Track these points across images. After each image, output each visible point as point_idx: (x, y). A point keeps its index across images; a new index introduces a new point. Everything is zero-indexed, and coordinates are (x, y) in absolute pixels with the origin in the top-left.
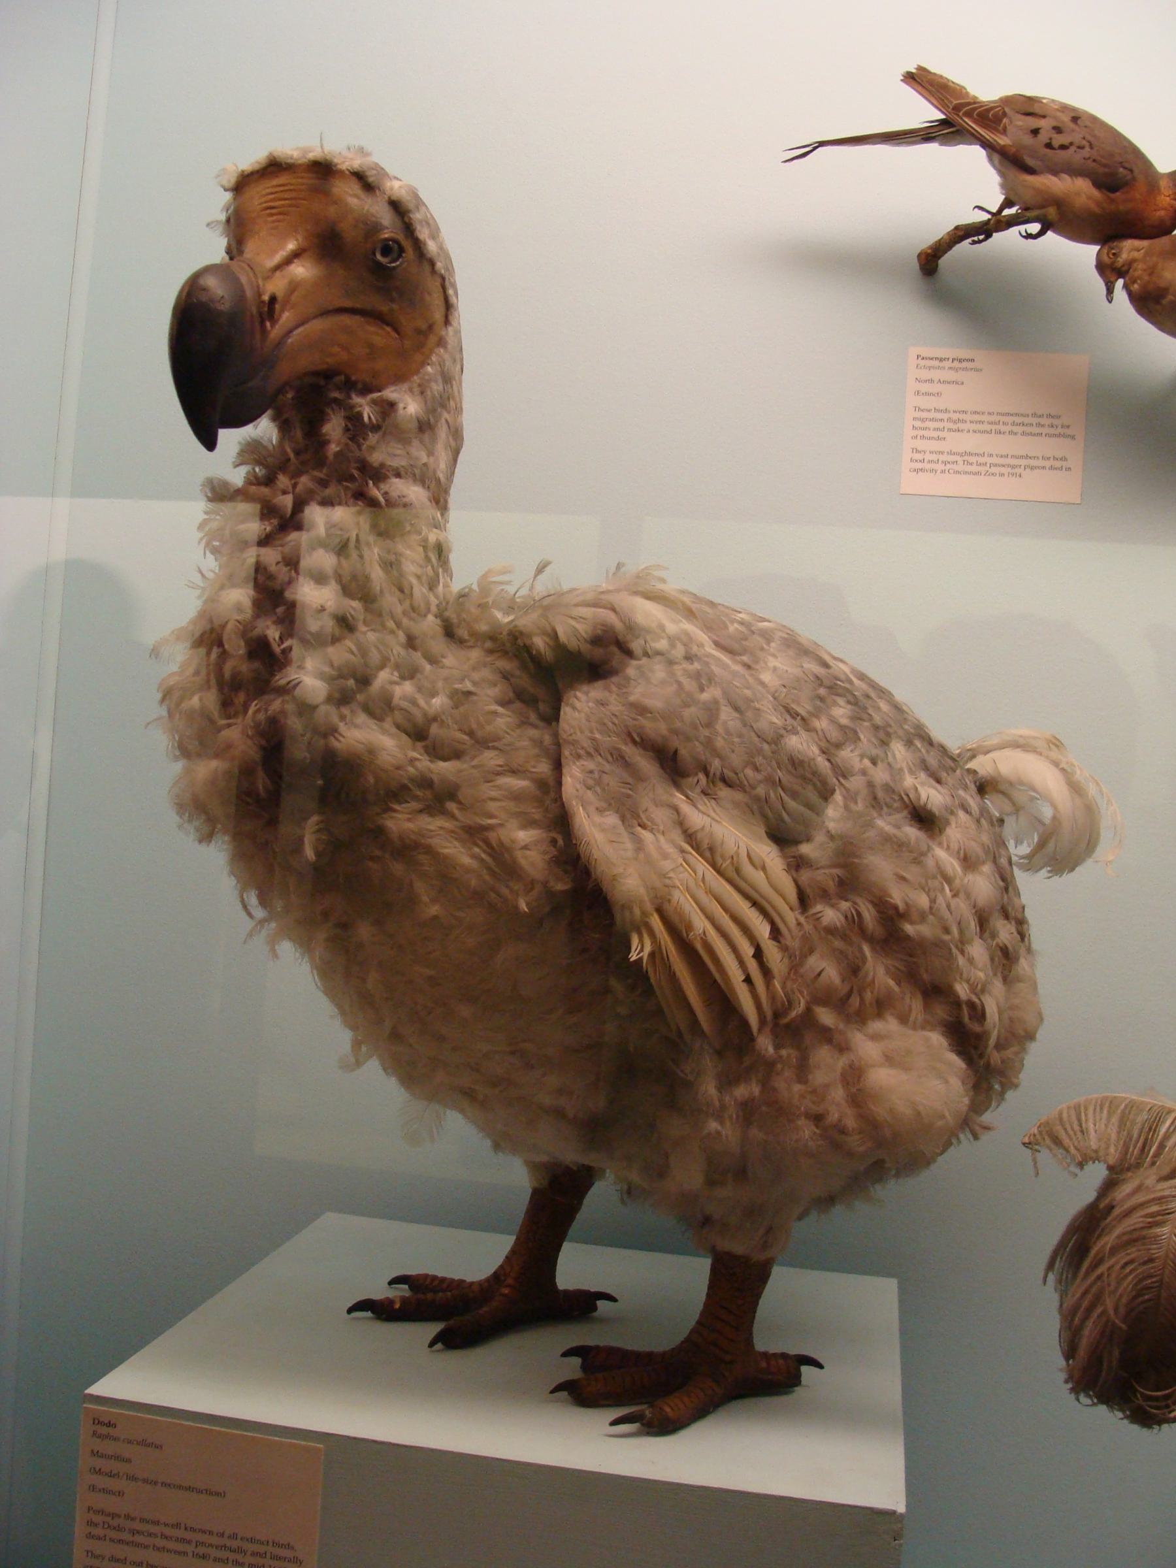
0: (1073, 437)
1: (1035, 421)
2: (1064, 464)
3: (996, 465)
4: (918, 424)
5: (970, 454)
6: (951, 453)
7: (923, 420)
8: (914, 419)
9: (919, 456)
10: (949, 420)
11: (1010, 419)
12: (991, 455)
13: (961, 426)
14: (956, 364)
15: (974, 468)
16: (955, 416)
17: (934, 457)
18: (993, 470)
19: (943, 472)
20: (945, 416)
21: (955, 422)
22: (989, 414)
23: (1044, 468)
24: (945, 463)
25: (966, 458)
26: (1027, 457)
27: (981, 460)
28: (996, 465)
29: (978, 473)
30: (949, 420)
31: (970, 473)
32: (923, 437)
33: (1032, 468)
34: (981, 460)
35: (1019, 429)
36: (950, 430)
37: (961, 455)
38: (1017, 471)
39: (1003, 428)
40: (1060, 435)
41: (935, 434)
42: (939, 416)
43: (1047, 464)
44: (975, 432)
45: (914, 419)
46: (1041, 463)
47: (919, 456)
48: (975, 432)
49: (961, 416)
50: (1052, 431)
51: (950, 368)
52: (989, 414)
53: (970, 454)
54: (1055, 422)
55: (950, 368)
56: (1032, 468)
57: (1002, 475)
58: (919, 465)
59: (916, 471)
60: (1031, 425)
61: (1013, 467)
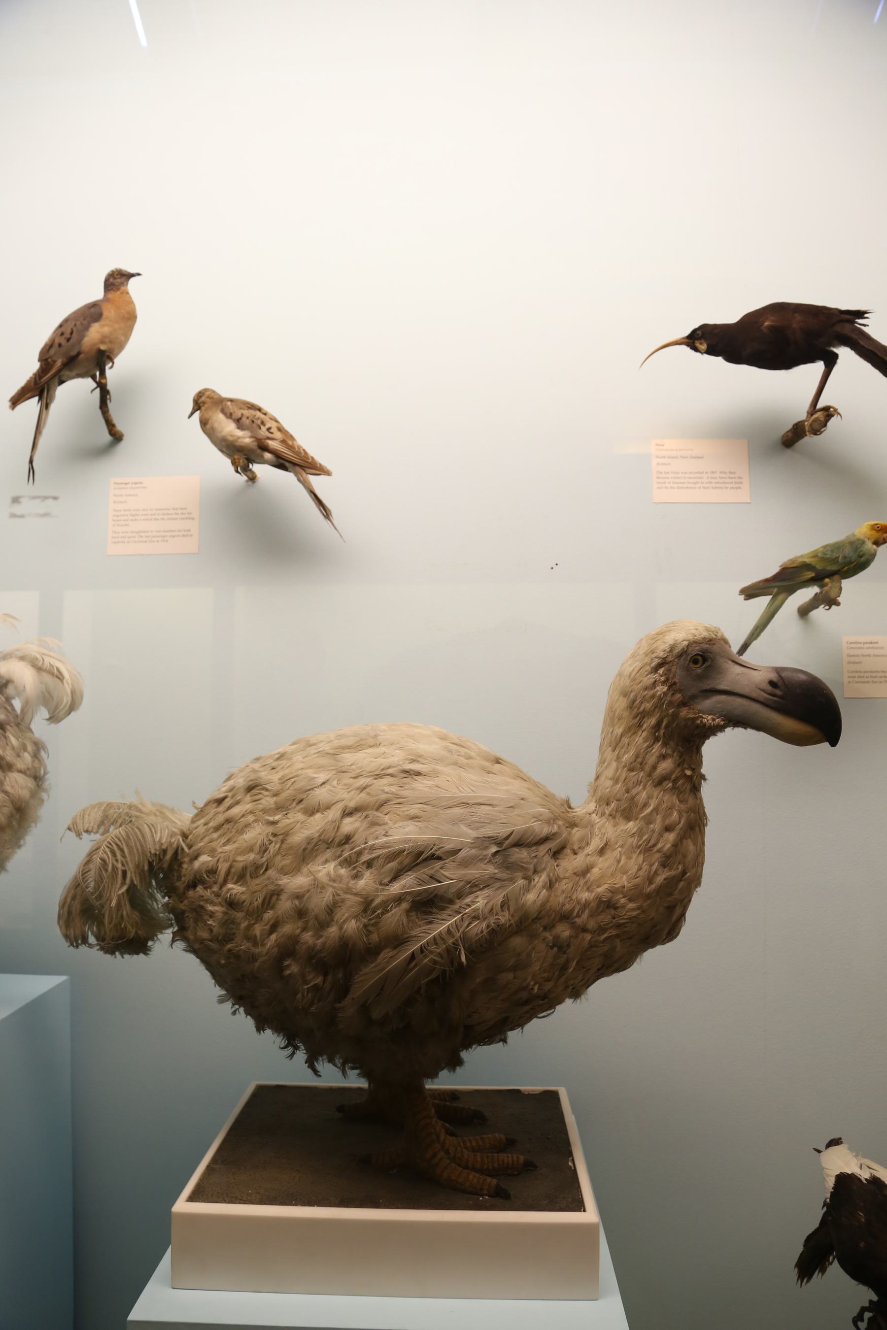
0: (193, 519)
1: (174, 512)
2: (189, 533)
3: (154, 537)
4: (115, 518)
5: (141, 532)
6: (132, 532)
7: (118, 516)
8: (114, 516)
9: (116, 535)
10: (131, 515)
11: (161, 512)
12: (152, 532)
13: (137, 517)
14: (134, 486)
15: (144, 539)
16: (134, 513)
17: (124, 535)
18: (154, 539)
19: (128, 542)
20: (128, 513)
21: (133, 515)
22: (151, 510)
23: (179, 536)
24: (129, 537)
25: (140, 534)
26: (170, 531)
27: (147, 534)
28: (154, 537)
29: (146, 542)
30: (131, 515)
31: (141, 542)
32: (118, 525)
33: (173, 536)
34: (147, 534)
35: (165, 517)
36: (131, 520)
37: (137, 533)
38: (166, 538)
39: (157, 517)
40: (186, 518)
41: (124, 523)
42: (126, 513)
43: (181, 534)
44: (144, 520)
45: (114, 516)
46: (177, 533)
47: (116, 535)
48: (144, 520)
49: (138, 513)
50: (183, 516)
51: (131, 488)
52: (151, 510)
53: (141, 532)
54: (184, 511)
55: (131, 488)
56: (173, 536)
57: (158, 541)
58: (116, 540)
59: (115, 543)
60: (172, 514)
61: (164, 537)
